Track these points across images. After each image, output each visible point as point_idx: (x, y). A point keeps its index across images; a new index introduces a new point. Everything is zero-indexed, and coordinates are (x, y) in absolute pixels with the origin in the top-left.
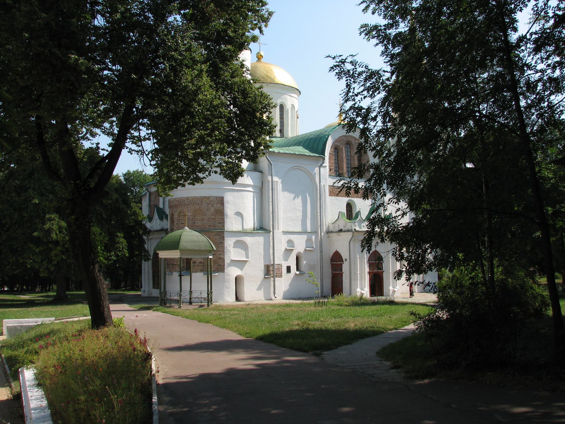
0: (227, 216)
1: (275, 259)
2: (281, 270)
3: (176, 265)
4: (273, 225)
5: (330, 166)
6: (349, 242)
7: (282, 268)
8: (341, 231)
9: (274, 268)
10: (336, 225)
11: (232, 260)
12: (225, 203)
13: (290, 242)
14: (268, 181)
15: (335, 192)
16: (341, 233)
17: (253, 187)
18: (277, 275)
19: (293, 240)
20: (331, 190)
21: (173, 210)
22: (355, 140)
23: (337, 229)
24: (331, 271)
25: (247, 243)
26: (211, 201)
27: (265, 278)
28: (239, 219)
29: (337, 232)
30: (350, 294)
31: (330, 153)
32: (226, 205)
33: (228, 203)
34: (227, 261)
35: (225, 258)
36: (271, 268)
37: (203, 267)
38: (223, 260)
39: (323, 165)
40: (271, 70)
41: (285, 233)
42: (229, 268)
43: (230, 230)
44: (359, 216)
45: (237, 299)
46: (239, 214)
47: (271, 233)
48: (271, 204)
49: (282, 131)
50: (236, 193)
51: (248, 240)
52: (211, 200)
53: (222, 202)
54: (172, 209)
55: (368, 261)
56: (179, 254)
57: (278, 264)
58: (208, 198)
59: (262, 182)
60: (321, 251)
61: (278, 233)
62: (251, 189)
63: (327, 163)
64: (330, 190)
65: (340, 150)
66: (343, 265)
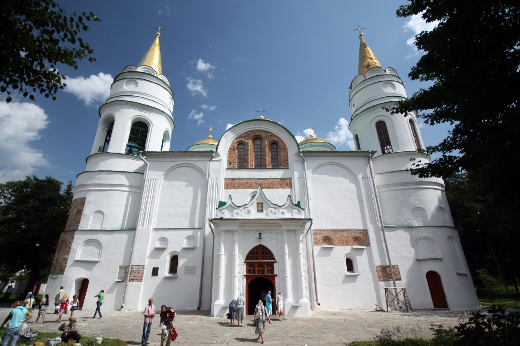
2: (141, 272)
5: (229, 161)
7: (145, 270)
15: (231, 184)
17: (130, 187)
18: (133, 278)
22: (266, 133)
31: (230, 149)
35: (69, 259)
38: (66, 260)
39: (213, 160)
50: (101, 193)
55: (247, 259)
57: (139, 266)
60: (204, 250)
62: (127, 189)
65: (245, 145)
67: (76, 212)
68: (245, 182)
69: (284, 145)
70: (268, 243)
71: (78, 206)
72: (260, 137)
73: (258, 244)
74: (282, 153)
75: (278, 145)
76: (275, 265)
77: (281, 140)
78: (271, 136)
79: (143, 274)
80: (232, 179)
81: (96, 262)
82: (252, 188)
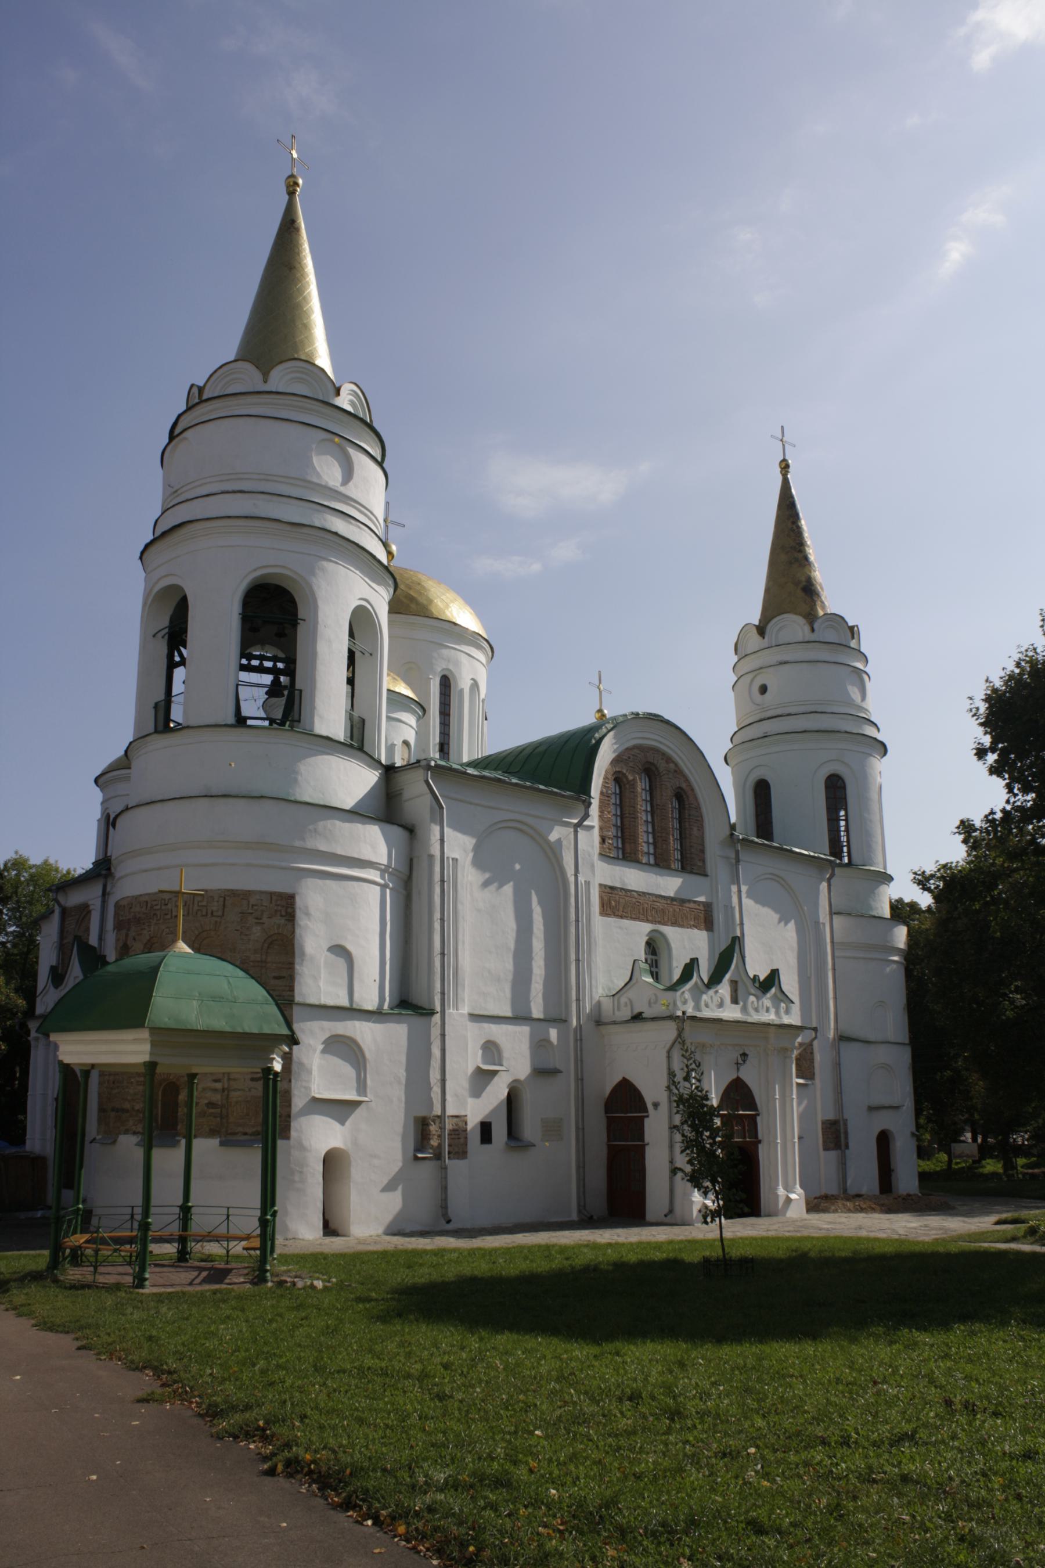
0: (303, 954)
1: (448, 1097)
3: (127, 1111)
4: (443, 993)
5: (601, 829)
6: (669, 1052)
8: (637, 1017)
9: (442, 1128)
10: (624, 1000)
11: (315, 1100)
12: (299, 914)
13: (491, 1049)
14: (431, 857)
16: (638, 1026)
17: (384, 871)
19: (498, 1041)
20: (606, 898)
21: (127, 935)
23: (626, 1014)
24: (606, 1140)
25: (361, 1044)
26: (253, 906)
27: (416, 1158)
28: (341, 963)
29: (627, 1022)
30: (671, 1211)
31: (602, 793)
32: (301, 920)
33: (308, 914)
34: (298, 1102)
36: (433, 1128)
37: (219, 1119)
39: (585, 823)
40: (419, 584)
41: (476, 1018)
42: (303, 1120)
43: (312, 1000)
44: (695, 975)
45: (329, 1229)
46: (340, 951)
47: (437, 1018)
48: (437, 926)
49: (446, 746)
51: (365, 1032)
52: (252, 901)
53: (290, 910)
54: (124, 932)
56: (147, 1047)
57: (457, 1117)
58: (246, 895)
59: (411, 860)
60: (580, 1080)
61: (457, 1016)
63: (594, 820)
64: (601, 898)
65: (627, 786)
66: (647, 1121)
67: (265, 941)
68: (634, 900)
69: (698, 808)
70: (750, 1076)
71: (265, 919)
72: (654, 769)
73: (735, 1076)
74: (695, 829)
75: (686, 803)
76: (759, 1119)
77: (693, 790)
78: (675, 771)
79: (466, 1138)
80: (612, 888)
81: (356, 1104)
82: (648, 921)
